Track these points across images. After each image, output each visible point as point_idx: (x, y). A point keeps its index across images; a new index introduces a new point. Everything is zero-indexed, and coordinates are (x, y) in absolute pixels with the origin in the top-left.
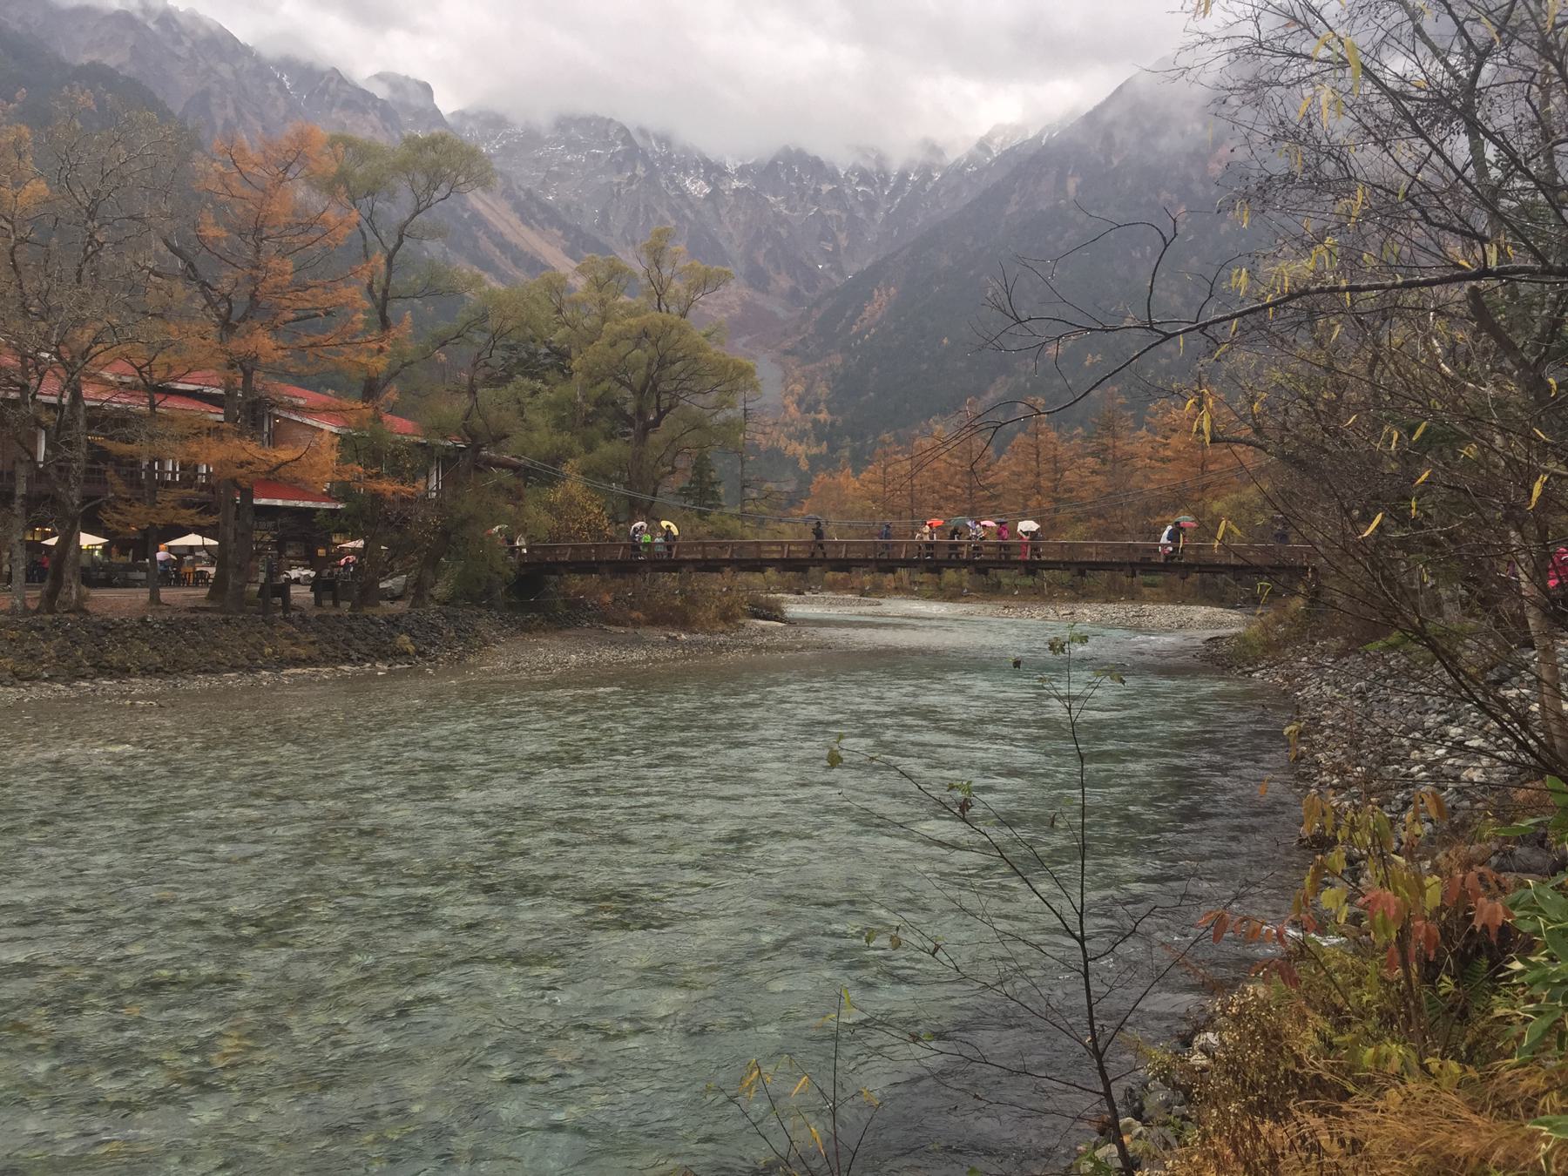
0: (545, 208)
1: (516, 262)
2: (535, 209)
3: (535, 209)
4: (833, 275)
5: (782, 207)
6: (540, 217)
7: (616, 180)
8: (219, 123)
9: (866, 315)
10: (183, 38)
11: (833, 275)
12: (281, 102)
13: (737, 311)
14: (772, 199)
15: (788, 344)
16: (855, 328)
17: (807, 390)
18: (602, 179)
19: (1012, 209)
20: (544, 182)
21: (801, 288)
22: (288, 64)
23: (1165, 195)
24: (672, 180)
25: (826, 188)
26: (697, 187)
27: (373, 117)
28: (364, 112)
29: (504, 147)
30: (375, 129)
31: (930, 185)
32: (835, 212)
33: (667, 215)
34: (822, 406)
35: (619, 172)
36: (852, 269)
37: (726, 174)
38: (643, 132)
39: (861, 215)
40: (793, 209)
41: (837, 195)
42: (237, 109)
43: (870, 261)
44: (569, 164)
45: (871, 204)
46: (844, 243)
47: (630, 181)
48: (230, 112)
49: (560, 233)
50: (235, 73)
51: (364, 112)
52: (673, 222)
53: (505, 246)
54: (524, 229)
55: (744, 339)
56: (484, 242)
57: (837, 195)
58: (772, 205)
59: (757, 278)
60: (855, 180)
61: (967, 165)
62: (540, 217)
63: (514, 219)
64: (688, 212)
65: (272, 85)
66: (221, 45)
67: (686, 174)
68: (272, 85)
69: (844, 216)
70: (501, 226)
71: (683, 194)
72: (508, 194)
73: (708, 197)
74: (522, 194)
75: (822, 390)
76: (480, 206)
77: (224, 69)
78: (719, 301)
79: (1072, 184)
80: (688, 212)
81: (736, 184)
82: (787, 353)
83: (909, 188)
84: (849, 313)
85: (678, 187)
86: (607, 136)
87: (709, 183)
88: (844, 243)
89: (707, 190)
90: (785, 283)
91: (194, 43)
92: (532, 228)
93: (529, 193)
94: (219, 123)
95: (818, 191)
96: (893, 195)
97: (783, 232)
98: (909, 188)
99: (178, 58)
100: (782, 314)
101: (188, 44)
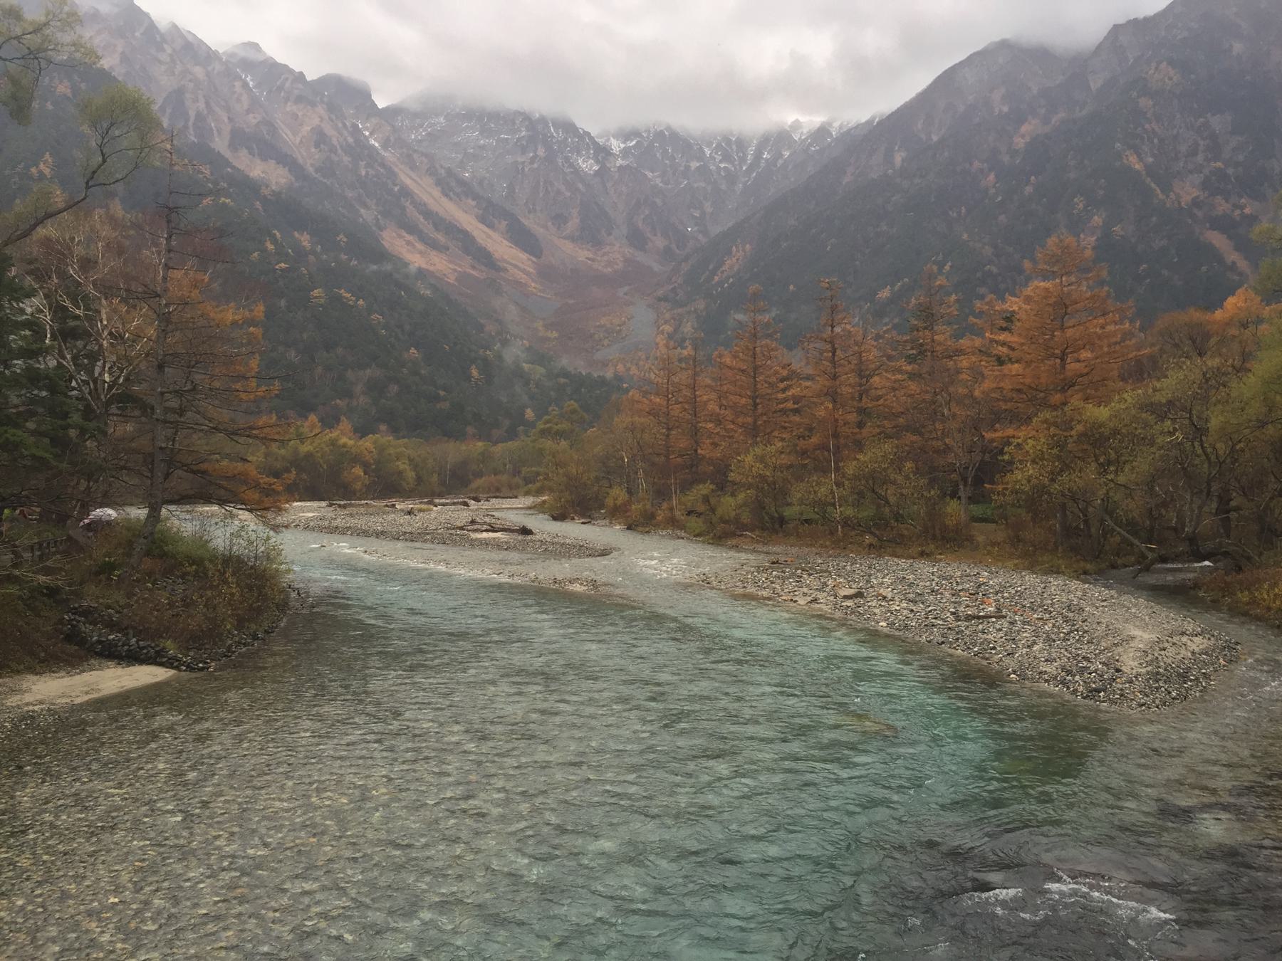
0: (462, 183)
1: (436, 227)
2: (453, 184)
3: (453, 184)
4: (700, 237)
5: (658, 181)
6: (458, 190)
7: (520, 160)
8: (192, 114)
9: (725, 267)
10: (165, 46)
11: (700, 237)
12: (245, 98)
13: (621, 265)
14: (650, 175)
15: (660, 293)
16: (716, 278)
17: (676, 330)
18: (509, 159)
19: (846, 180)
20: (462, 162)
21: (673, 246)
22: (247, 65)
23: (977, 164)
24: (567, 159)
25: (694, 165)
26: (587, 165)
27: (321, 110)
28: (313, 105)
29: (429, 134)
30: (322, 119)
31: (780, 162)
32: (703, 184)
33: (563, 188)
34: (687, 343)
35: (524, 150)
36: (715, 230)
37: (611, 154)
38: (543, 120)
39: (723, 187)
40: (666, 183)
41: (703, 170)
42: (207, 103)
43: (730, 224)
44: (482, 147)
45: (731, 178)
46: (709, 209)
47: (532, 161)
48: (201, 105)
49: (474, 203)
50: (208, 75)
51: (313, 105)
52: (568, 194)
53: (428, 214)
54: (444, 200)
55: (626, 288)
56: (411, 211)
57: (703, 170)
58: (650, 180)
59: (637, 239)
60: (718, 158)
61: (811, 145)
62: (458, 190)
63: (436, 192)
64: (580, 186)
65: (238, 84)
66: (191, 49)
67: (579, 153)
68: (238, 84)
69: (709, 188)
70: (425, 198)
71: (577, 171)
72: (431, 171)
73: (597, 173)
74: (443, 171)
75: (688, 328)
76: (408, 182)
77: (199, 71)
78: (605, 258)
79: (898, 158)
80: (580, 186)
81: (620, 162)
82: (660, 299)
83: (763, 164)
84: (711, 267)
85: (571, 165)
86: (514, 123)
87: (597, 162)
88: (708, 208)
89: (596, 168)
90: (660, 242)
91: (174, 50)
92: (451, 199)
93: (450, 172)
94: (192, 114)
95: (688, 168)
96: (751, 168)
97: (658, 201)
98: (763, 164)
99: (160, 62)
100: (657, 267)
101: (169, 51)
